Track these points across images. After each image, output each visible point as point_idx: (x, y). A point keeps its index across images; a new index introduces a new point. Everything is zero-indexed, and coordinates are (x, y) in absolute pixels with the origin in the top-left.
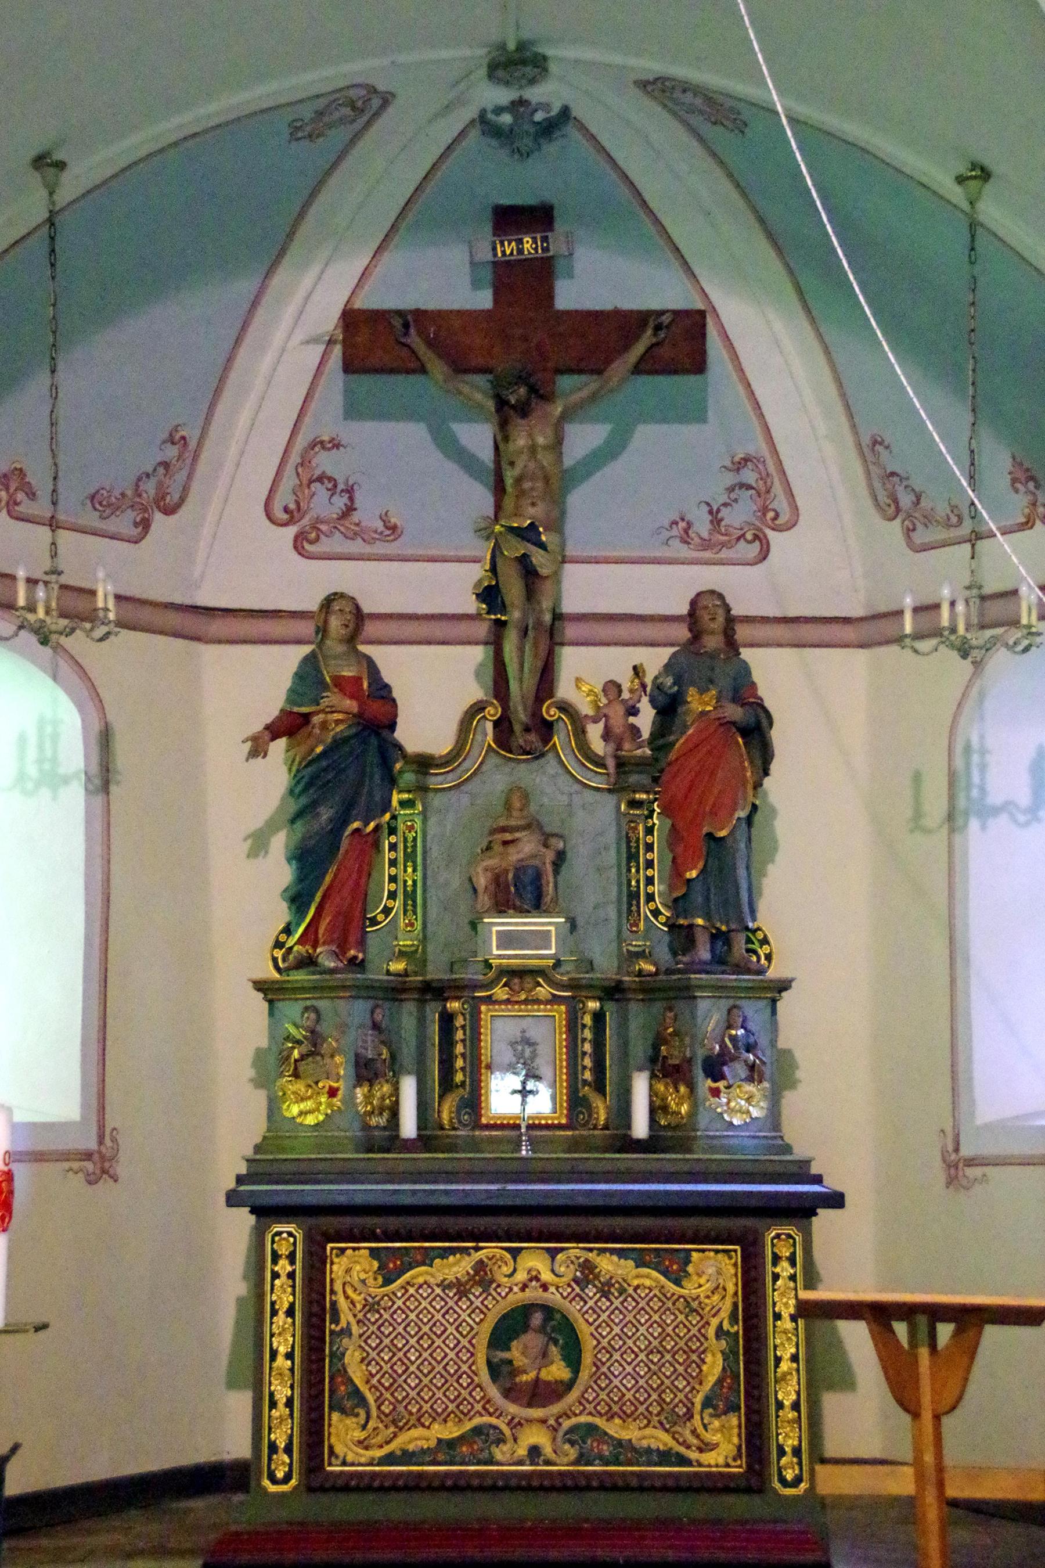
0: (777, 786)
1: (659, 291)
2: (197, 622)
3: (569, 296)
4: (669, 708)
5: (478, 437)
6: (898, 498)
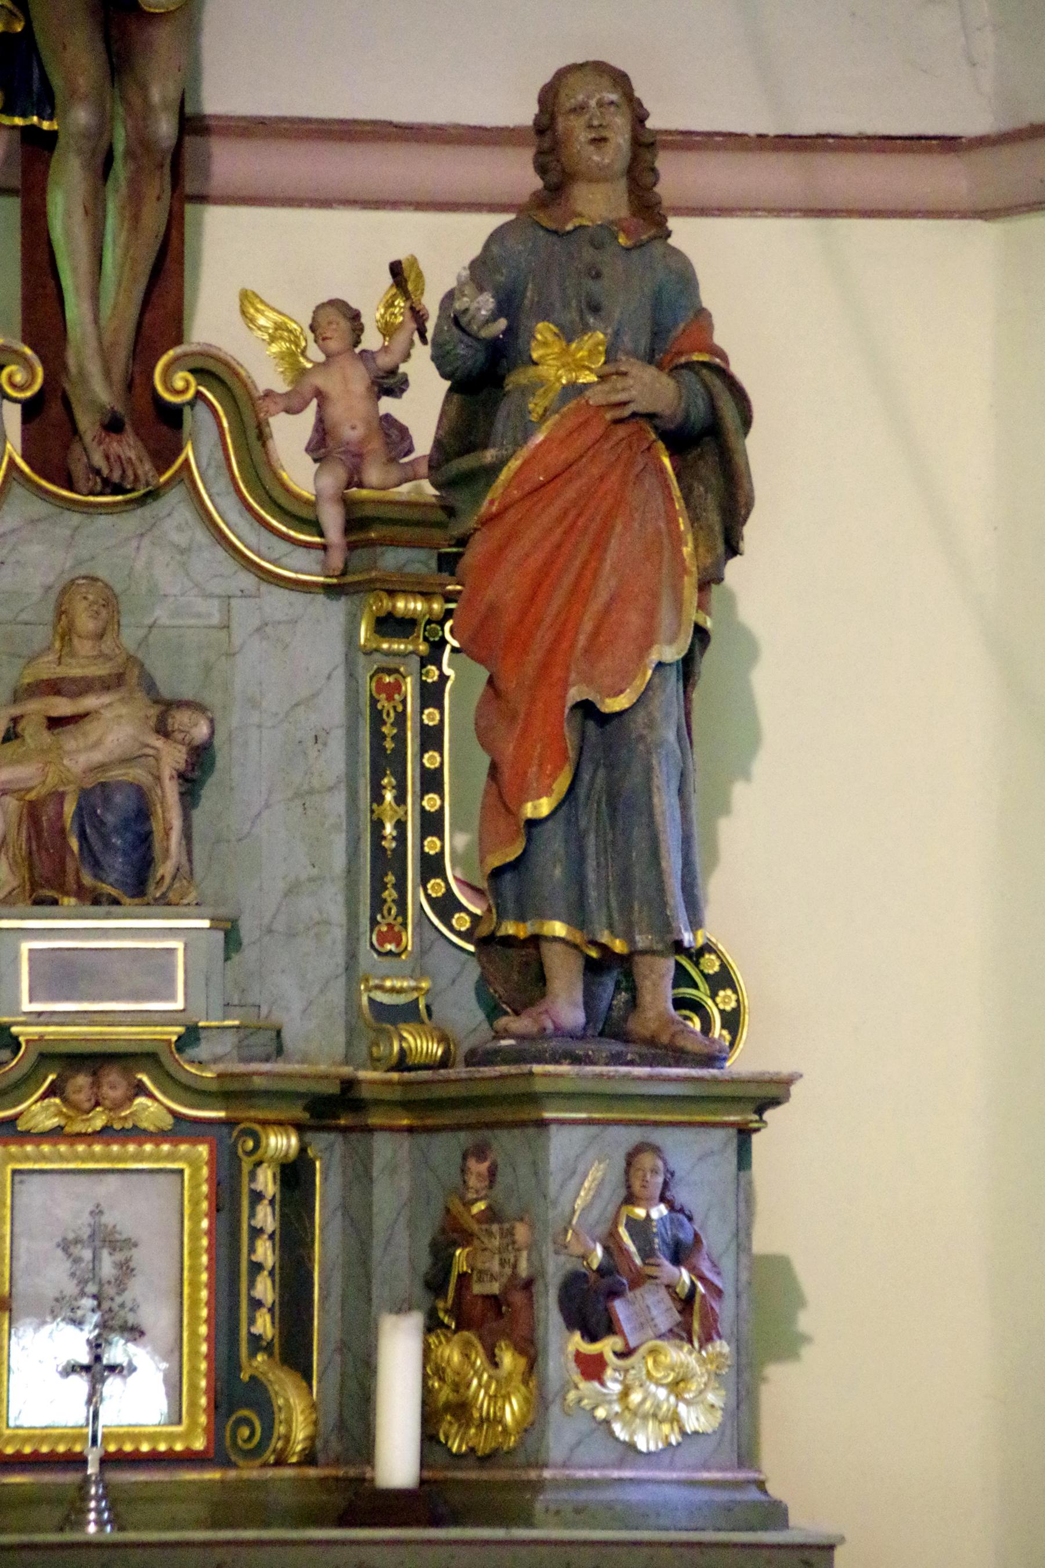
4: (483, 378)
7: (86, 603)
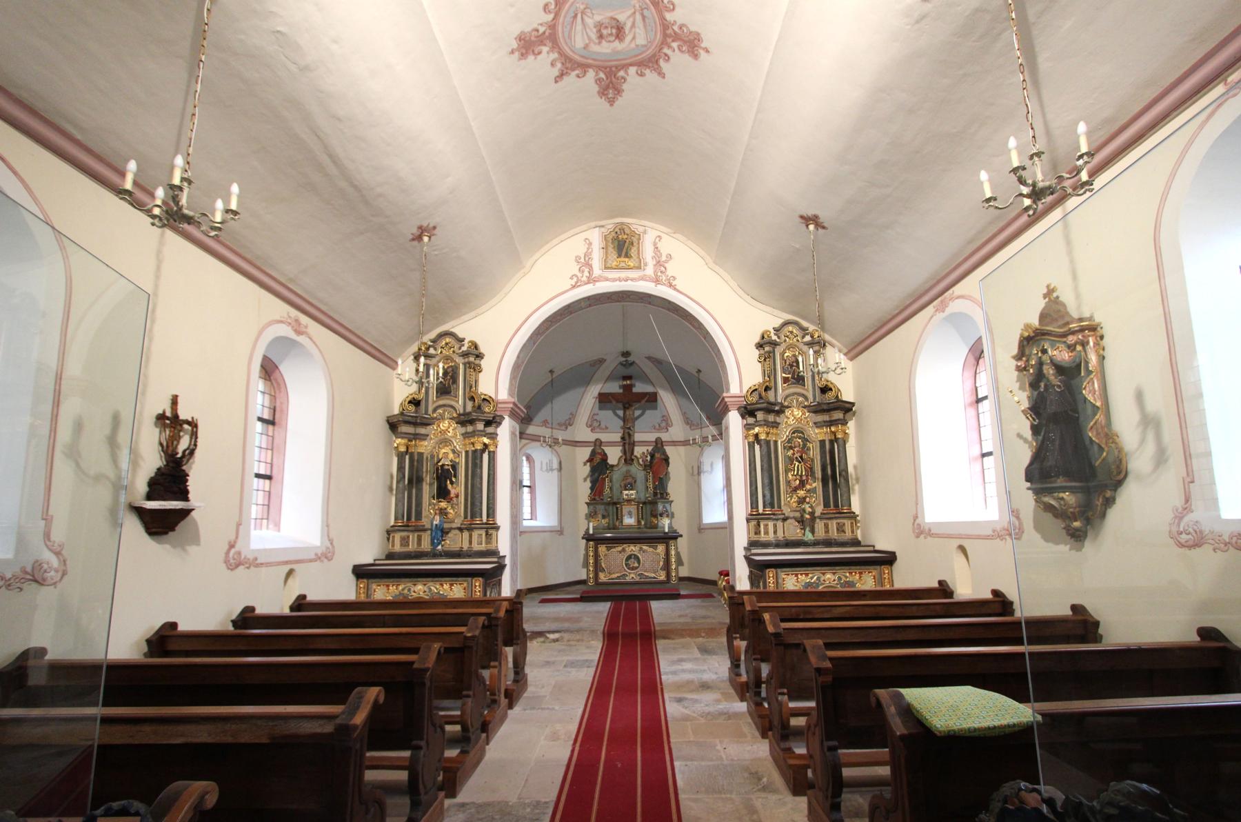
0: (670, 469)
1: (649, 389)
2: (575, 444)
3: (635, 390)
4: (652, 456)
5: (621, 413)
6: (688, 422)
7: (628, 471)
